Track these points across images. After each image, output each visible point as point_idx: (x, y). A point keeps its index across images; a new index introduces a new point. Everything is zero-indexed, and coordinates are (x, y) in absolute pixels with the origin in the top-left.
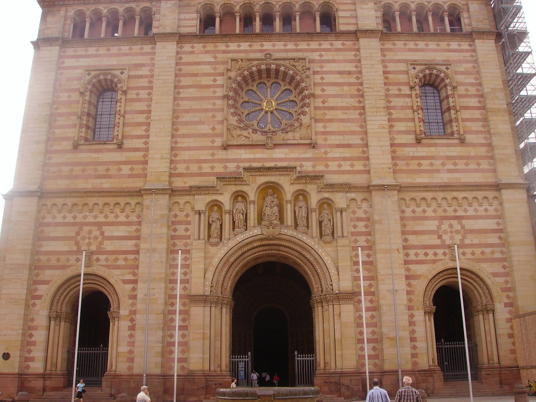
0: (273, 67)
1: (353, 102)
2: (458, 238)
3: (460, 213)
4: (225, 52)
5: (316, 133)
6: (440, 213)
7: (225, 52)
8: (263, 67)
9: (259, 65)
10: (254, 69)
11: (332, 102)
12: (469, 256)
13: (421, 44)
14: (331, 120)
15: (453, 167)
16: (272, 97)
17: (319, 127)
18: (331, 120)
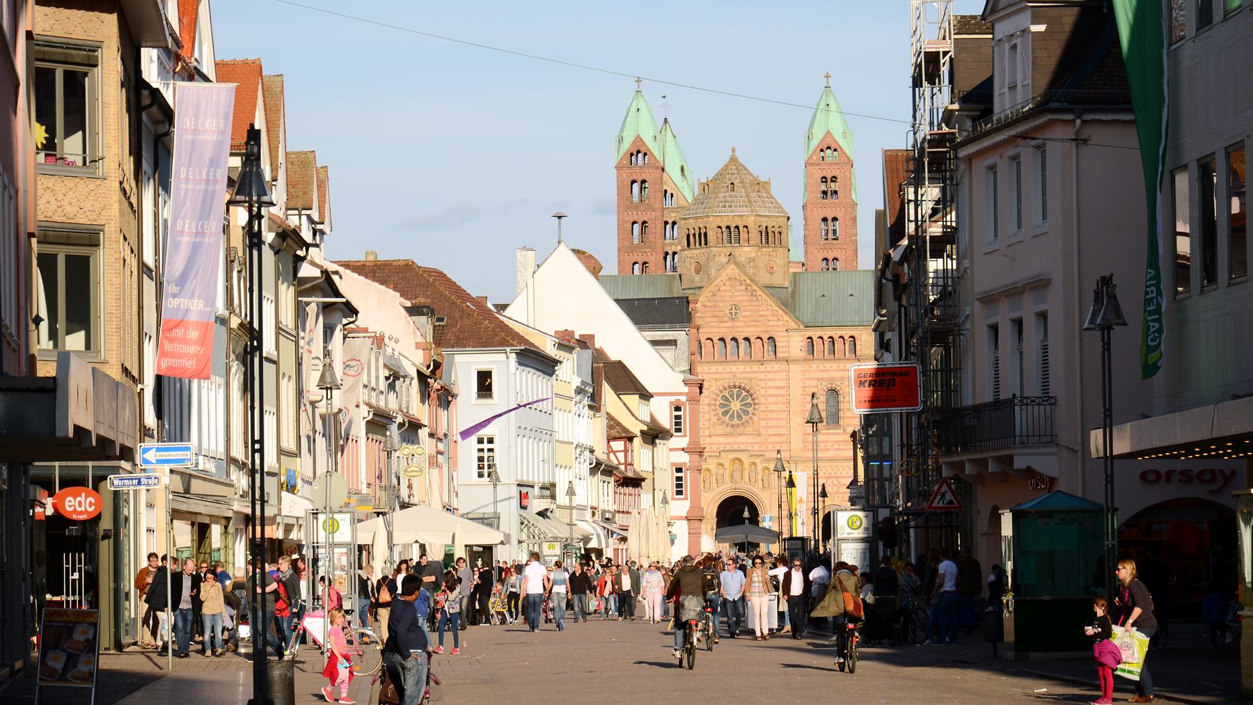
0: (737, 384)
1: (783, 407)
2: (835, 489)
3: (838, 475)
4: (708, 373)
5: (762, 427)
6: (827, 475)
7: (708, 373)
8: (732, 384)
9: (729, 383)
10: (726, 385)
11: (771, 407)
12: (841, 498)
13: (828, 366)
14: (770, 419)
15: (837, 447)
16: (737, 399)
17: (763, 423)
18: (770, 419)
